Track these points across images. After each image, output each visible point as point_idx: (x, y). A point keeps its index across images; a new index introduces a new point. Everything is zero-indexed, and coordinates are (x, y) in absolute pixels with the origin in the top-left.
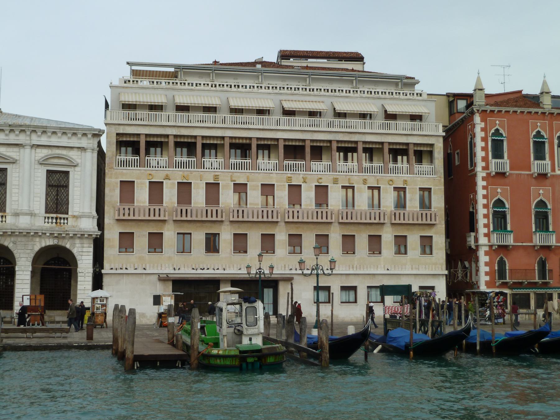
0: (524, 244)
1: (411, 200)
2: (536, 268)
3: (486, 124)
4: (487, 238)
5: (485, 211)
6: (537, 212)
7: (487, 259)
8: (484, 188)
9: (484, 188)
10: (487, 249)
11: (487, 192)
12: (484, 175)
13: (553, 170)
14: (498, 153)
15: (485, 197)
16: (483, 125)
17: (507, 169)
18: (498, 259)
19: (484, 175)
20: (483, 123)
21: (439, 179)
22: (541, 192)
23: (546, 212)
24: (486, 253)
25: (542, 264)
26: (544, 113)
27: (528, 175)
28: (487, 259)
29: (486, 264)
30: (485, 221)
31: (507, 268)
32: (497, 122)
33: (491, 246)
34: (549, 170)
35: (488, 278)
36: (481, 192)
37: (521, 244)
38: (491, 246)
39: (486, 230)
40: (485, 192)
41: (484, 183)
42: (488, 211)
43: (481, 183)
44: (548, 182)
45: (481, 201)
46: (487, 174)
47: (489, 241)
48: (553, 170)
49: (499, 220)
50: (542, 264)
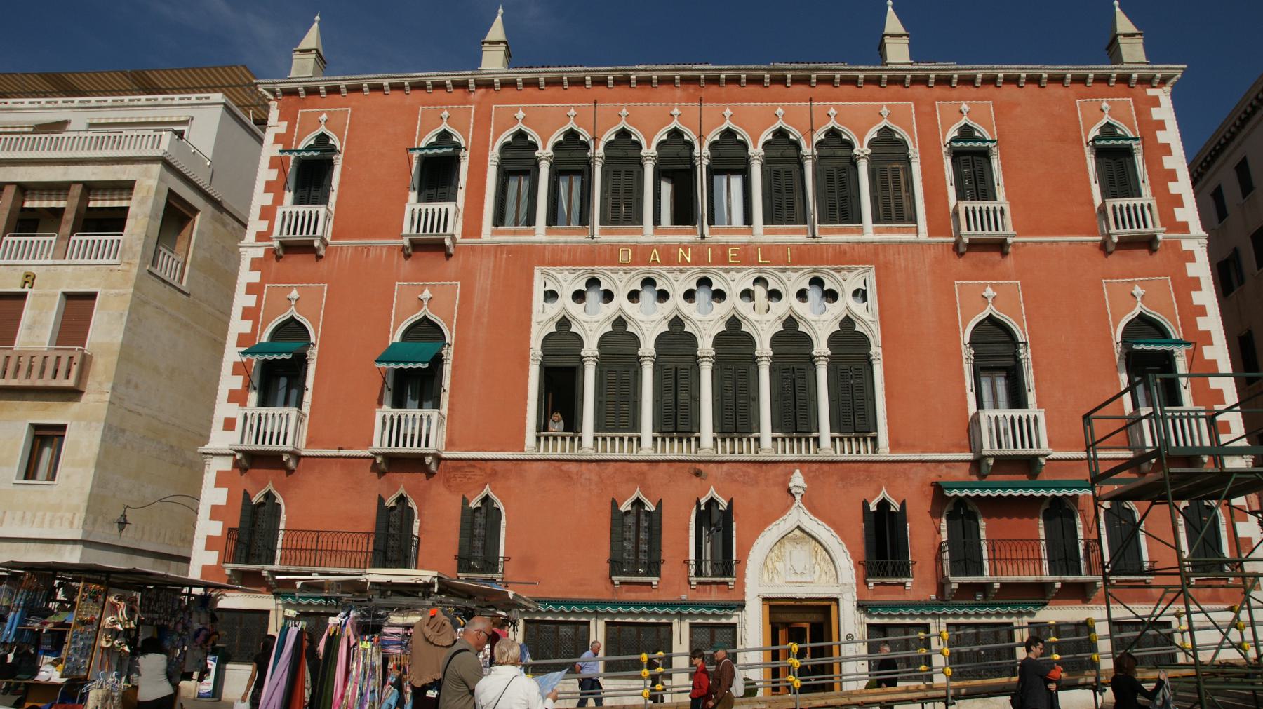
1: (30, 328)
3: (291, 128)
8: (251, 288)
9: (251, 288)
10: (226, 465)
13: (472, 228)
15: (247, 314)
16: (283, 128)
17: (325, 229)
19: (260, 253)
20: (285, 124)
21: (127, 267)
24: (221, 480)
29: (216, 513)
31: (282, 526)
34: (455, 227)
36: (243, 300)
37: (334, 452)
40: (251, 301)
41: (255, 277)
43: (247, 276)
46: (267, 251)
48: (472, 228)
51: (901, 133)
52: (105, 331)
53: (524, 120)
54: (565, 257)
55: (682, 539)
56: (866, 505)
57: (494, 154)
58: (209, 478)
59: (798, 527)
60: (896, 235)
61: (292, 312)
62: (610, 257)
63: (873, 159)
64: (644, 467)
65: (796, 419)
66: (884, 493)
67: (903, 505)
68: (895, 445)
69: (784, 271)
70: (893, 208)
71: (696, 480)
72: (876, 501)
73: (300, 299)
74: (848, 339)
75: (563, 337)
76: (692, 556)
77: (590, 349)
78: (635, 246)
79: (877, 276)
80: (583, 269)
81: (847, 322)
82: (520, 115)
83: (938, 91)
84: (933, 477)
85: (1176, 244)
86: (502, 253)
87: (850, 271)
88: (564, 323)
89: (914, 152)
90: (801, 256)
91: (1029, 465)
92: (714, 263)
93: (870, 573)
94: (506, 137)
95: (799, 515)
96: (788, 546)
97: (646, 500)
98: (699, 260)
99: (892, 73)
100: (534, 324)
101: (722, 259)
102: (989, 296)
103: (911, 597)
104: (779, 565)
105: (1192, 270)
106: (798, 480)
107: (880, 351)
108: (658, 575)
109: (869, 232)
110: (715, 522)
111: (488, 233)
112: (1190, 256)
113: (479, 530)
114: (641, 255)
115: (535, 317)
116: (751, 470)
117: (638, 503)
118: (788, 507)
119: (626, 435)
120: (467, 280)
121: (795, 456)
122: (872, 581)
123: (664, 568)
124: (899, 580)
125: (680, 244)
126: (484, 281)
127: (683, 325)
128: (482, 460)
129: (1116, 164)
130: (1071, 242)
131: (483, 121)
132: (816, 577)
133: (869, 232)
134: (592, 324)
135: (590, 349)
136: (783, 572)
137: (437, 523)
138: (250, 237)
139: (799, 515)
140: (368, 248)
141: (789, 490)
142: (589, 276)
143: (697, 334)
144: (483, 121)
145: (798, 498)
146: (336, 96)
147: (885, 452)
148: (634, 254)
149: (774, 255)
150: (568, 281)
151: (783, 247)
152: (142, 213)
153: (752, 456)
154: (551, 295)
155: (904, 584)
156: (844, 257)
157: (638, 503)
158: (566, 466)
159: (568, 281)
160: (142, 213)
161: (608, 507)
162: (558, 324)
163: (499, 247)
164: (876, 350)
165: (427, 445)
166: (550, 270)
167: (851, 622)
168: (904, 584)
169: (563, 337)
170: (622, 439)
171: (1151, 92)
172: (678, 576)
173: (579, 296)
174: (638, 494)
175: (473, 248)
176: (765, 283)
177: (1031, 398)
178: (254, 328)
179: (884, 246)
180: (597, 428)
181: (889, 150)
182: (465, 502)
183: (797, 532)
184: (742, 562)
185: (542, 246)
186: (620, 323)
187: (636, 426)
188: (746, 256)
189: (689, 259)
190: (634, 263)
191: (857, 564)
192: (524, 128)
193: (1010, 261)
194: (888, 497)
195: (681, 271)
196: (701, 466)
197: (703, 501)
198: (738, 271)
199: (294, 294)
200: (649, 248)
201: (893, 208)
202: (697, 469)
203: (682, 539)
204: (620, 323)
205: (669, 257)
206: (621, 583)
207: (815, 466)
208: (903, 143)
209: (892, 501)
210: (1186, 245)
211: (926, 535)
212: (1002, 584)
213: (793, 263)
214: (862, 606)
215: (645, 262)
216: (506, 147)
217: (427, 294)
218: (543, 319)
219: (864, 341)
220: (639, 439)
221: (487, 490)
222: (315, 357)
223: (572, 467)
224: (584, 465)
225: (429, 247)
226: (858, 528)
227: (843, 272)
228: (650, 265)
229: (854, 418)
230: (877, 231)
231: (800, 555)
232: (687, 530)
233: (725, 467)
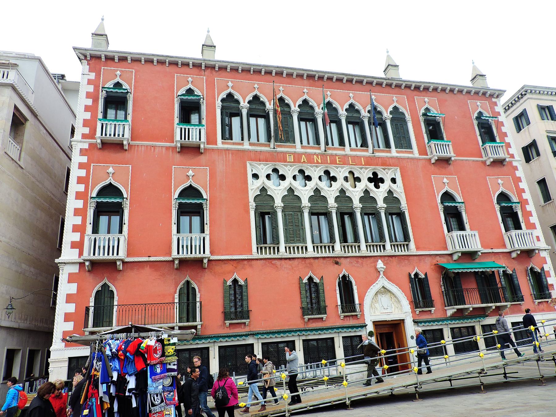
0: (152, 259)
2: (177, 300)
4: (77, 250)
5: (80, 204)
6: (180, 204)
7: (73, 288)
8: (81, 166)
9: (81, 166)
10: (75, 269)
11: (88, 173)
12: (86, 146)
13: (211, 140)
15: (80, 180)
17: (127, 135)
18: (98, 287)
19: (86, 146)
23: (201, 204)
24: (72, 278)
25: (188, 294)
27: (167, 148)
28: (73, 288)
29: (70, 298)
30: (78, 220)
32: (118, 73)
33: (82, 264)
35: (70, 326)
38: (82, 264)
39: (76, 237)
40: (83, 173)
41: (84, 159)
42: (85, 204)
43: (77, 158)
44: (203, 158)
45: (74, 187)
46: (90, 145)
47: (81, 254)
48: (211, 140)
50: (188, 294)
51: (402, 109)
53: (232, 87)
54: (262, 157)
55: (333, 297)
56: (410, 275)
57: (219, 104)
58: (63, 278)
59: (383, 287)
60: (404, 155)
62: (283, 158)
63: (392, 120)
64: (312, 261)
66: (416, 270)
67: (426, 275)
68: (418, 248)
69: (361, 168)
70: (403, 142)
71: (336, 266)
72: (414, 273)
73: (111, 173)
76: (339, 303)
77: (278, 203)
78: (294, 154)
79: (400, 172)
80: (270, 164)
81: (390, 192)
82: (230, 84)
83: (416, 93)
84: (435, 262)
85: (511, 163)
86: (229, 154)
87: (389, 169)
89: (408, 117)
90: (369, 161)
91: (470, 256)
92: (331, 163)
93: (417, 307)
94: (223, 95)
95: (383, 281)
96: (379, 296)
97: (314, 277)
98: (324, 162)
99: (397, 82)
100: (250, 190)
101: (333, 162)
102: (445, 182)
103: (434, 317)
104: (377, 305)
106: (380, 264)
107: (406, 205)
108: (325, 313)
109: (394, 152)
111: (220, 143)
114: (297, 158)
115: (250, 187)
116: (360, 260)
117: (310, 279)
118: (378, 277)
119: (300, 245)
121: (379, 254)
122: (418, 311)
123: (328, 310)
124: (429, 309)
125: (315, 154)
127: (320, 193)
128: (231, 260)
130: (473, 161)
131: (211, 85)
132: (393, 310)
134: (278, 191)
135: (278, 203)
136: (379, 308)
137: (210, 294)
139: (383, 281)
140: (154, 147)
141: (376, 269)
142: (273, 167)
143: (327, 196)
144: (211, 85)
145: (382, 273)
146: (124, 63)
148: (294, 157)
149: (356, 160)
150: (263, 169)
151: (359, 157)
153: (357, 254)
154: (256, 176)
155: (430, 311)
156: (386, 163)
157: (310, 279)
158: (274, 262)
159: (263, 169)
161: (296, 281)
162: (261, 190)
163: (227, 150)
165: (204, 253)
166: (254, 163)
167: (411, 330)
168: (430, 311)
170: (298, 248)
171: (494, 100)
173: (268, 177)
174: (310, 274)
175: (213, 150)
176: (353, 174)
177: (467, 226)
178: (87, 188)
180: (286, 241)
182: (225, 282)
183: (382, 289)
184: (361, 305)
185: (249, 151)
186: (291, 190)
187: (304, 241)
188: (344, 160)
189: (320, 161)
190: (294, 162)
191: (411, 302)
192: (232, 91)
193: (451, 168)
194: (418, 271)
195: (317, 167)
196: (338, 260)
197: (341, 276)
198: (342, 168)
199: (111, 170)
200: (300, 155)
201: (403, 142)
202: (336, 261)
203: (333, 297)
204: (291, 190)
205: (310, 159)
206: (309, 319)
207: (387, 258)
208: (403, 114)
209: (420, 273)
210: (515, 164)
211: (436, 289)
212: (473, 308)
213: (365, 165)
214: (416, 322)
215: (300, 162)
216: (223, 100)
217: (191, 173)
218: (254, 187)
219: (397, 200)
220: (306, 248)
221: (235, 276)
222: (128, 206)
223: (278, 263)
224: (283, 261)
226: (408, 286)
227: (386, 170)
228: (302, 163)
230: (397, 152)
231: (385, 299)
232: (335, 290)
233: (348, 260)
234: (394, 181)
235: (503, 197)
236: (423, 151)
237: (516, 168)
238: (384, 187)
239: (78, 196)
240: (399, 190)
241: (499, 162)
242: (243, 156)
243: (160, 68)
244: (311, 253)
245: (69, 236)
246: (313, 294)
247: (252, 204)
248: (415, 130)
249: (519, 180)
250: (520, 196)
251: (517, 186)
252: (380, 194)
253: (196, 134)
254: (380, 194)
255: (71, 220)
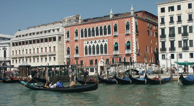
8: (65, 45)
9: (65, 45)
13: (79, 38)
14: (68, 37)
15: (66, 47)
16: (65, 30)
22: (77, 44)
26: (79, 25)
36: (65, 46)
49: (68, 52)
51: (110, 25)
52: (56, 49)
55: (94, 62)
57: (80, 31)
61: (68, 46)
65: (102, 52)
68: (108, 54)
70: (109, 33)
74: (106, 45)
75: (86, 47)
81: (106, 44)
88: (86, 46)
89: (111, 27)
95: (102, 60)
105: (133, 36)
106: (102, 57)
110: (96, 61)
111: (81, 38)
112: (133, 35)
113: (82, 62)
114: (92, 39)
120: (79, 42)
126: (80, 43)
129: (128, 27)
133: (107, 35)
134: (88, 46)
138: (65, 41)
147: (108, 54)
152: (57, 39)
156: (105, 38)
160: (57, 39)
164: (107, 46)
169: (86, 47)
172: (94, 65)
179: (108, 36)
180: (89, 54)
181: (109, 27)
201: (109, 33)
202: (95, 56)
203: (94, 62)
210: (133, 34)
218: (85, 45)
225: (76, 41)
229: (106, 52)
234: (107, 41)
235: (128, 42)
236: (112, 34)
237: (133, 35)
238: (104, 43)
239: (66, 49)
240: (107, 43)
241: (128, 35)
242: (83, 40)
243: (73, 27)
244: (92, 55)
245: (65, 55)
246: (91, 62)
247: (84, 48)
248: (112, 29)
249: (133, 37)
250: (132, 41)
251: (132, 39)
252: (104, 44)
253: (77, 38)
254: (104, 44)
255: (65, 52)
